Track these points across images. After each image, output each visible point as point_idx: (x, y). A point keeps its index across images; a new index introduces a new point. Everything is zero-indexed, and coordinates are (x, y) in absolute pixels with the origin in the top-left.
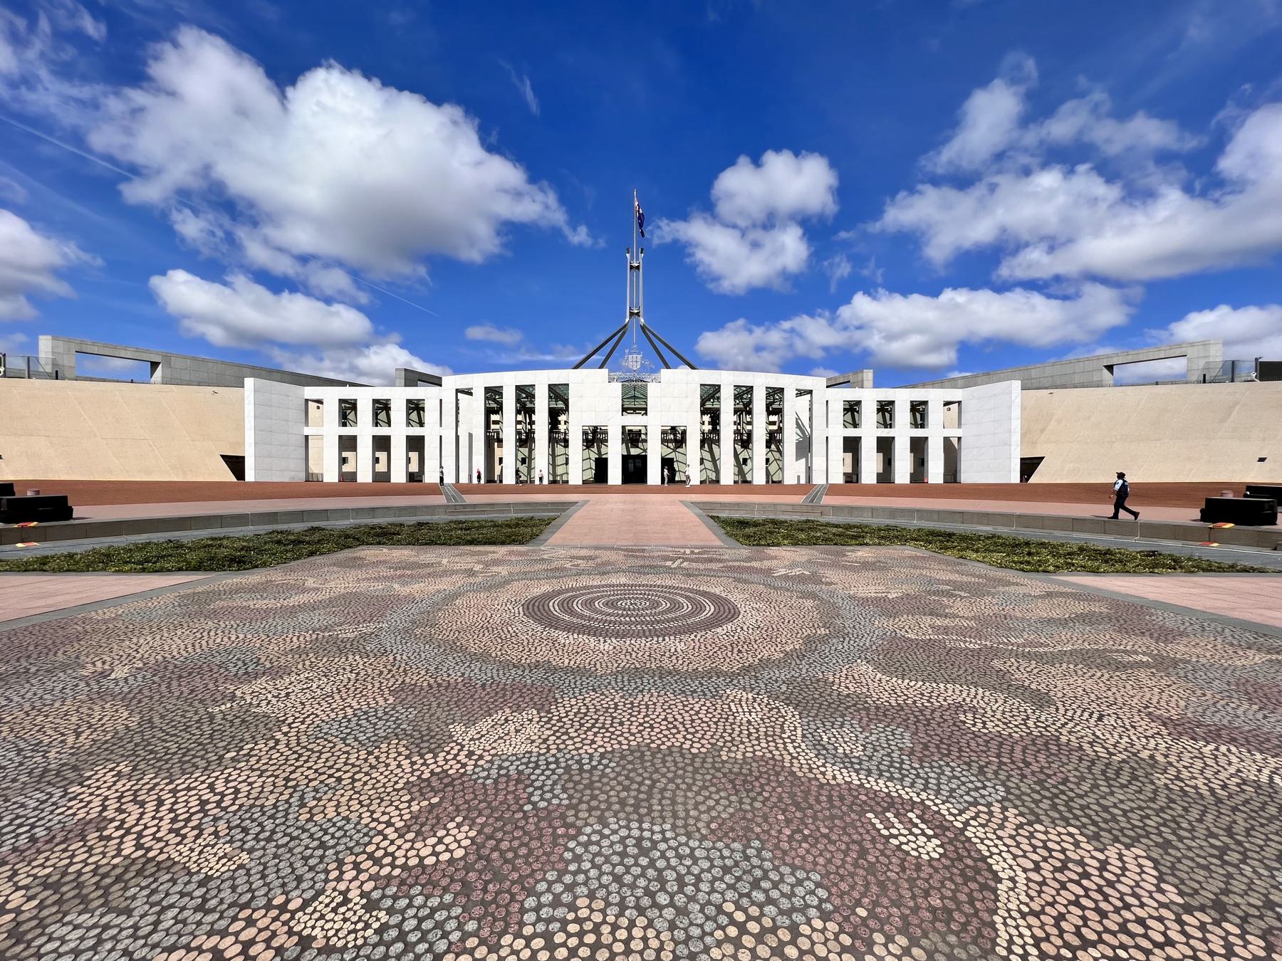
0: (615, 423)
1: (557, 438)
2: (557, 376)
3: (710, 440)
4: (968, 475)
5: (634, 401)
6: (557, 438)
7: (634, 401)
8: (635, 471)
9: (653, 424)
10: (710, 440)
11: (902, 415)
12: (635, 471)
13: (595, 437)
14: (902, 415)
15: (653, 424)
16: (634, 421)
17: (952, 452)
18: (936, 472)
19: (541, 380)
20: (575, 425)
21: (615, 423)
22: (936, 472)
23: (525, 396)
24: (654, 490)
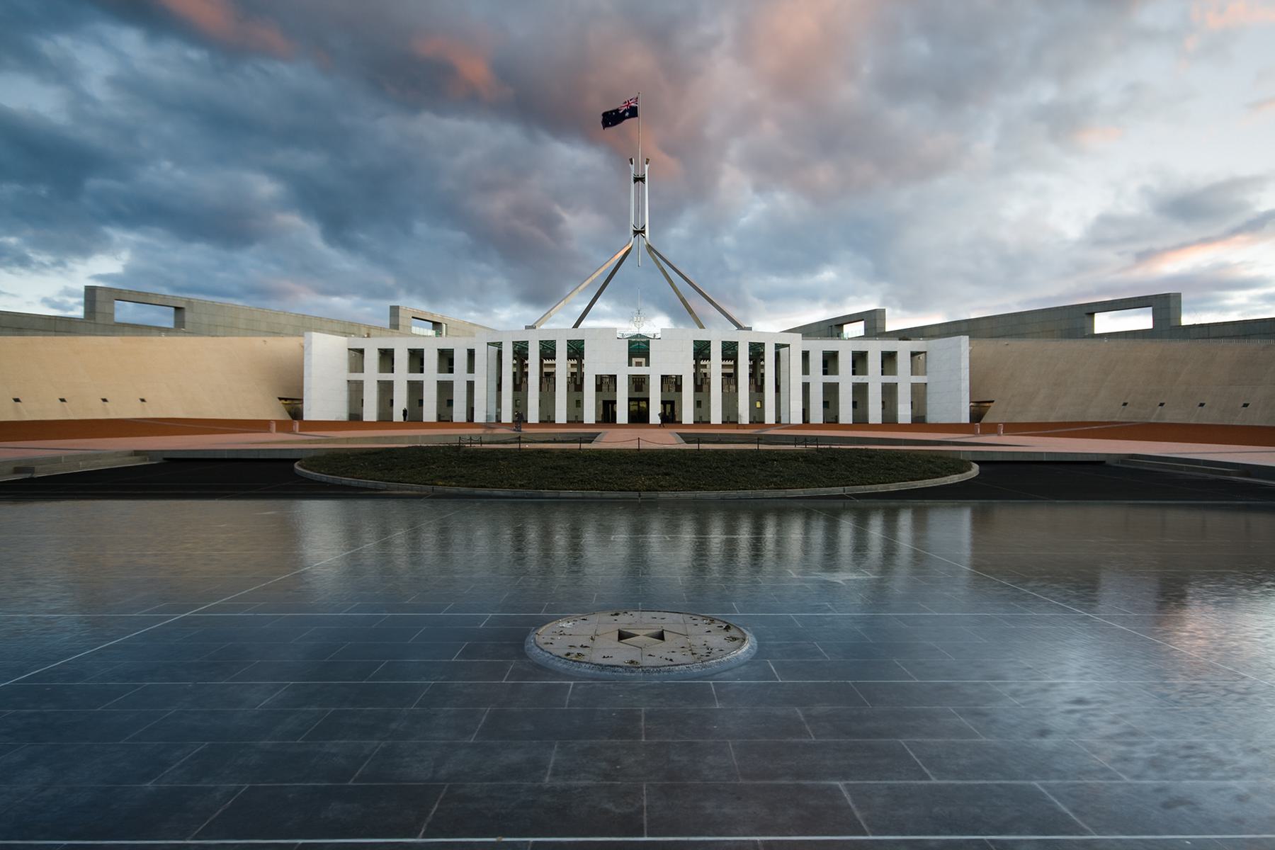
0: (624, 372)
1: (576, 383)
3: (701, 384)
6: (576, 383)
9: (654, 372)
11: (874, 363)
13: (606, 383)
14: (874, 363)
15: (654, 372)
17: (919, 393)
18: (904, 413)
21: (624, 372)
24: (655, 426)
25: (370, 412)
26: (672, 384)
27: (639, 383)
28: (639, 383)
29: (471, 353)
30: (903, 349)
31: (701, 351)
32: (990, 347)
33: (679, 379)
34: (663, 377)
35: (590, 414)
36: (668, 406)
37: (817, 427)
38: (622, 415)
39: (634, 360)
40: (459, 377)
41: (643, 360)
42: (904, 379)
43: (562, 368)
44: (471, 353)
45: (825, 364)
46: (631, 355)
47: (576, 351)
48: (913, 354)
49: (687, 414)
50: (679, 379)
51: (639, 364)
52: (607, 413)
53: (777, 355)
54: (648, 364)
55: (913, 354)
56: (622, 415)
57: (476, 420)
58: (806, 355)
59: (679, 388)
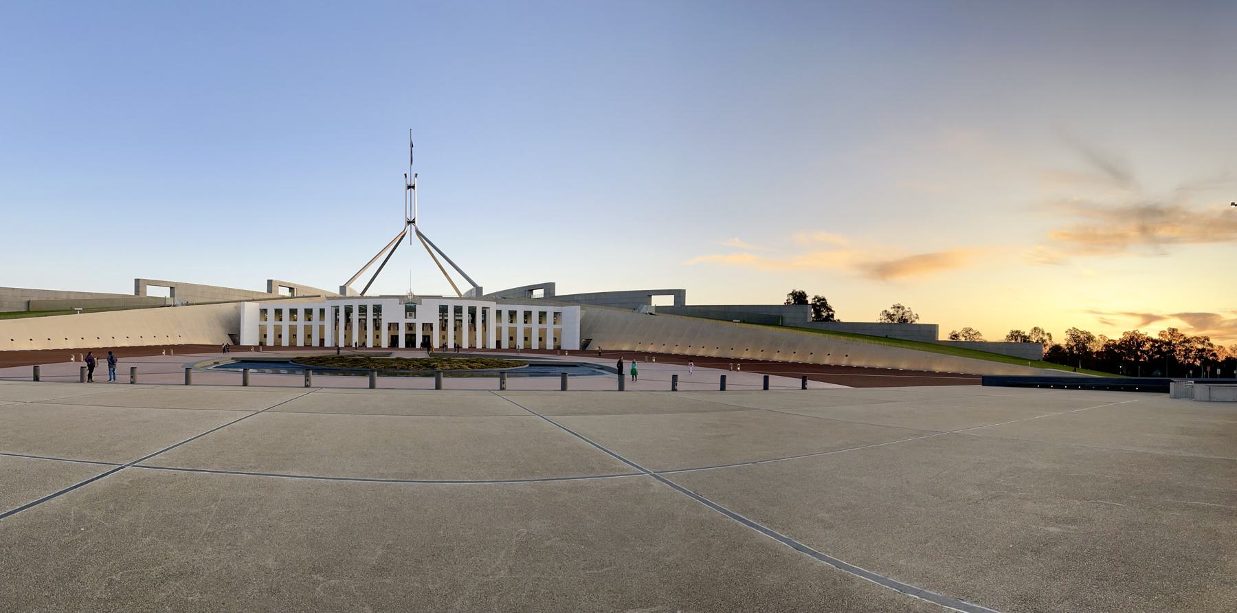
1: (377, 327)
3: (444, 327)
5: (410, 310)
6: (377, 327)
7: (410, 310)
8: (410, 342)
9: (418, 322)
10: (444, 327)
12: (410, 342)
13: (393, 326)
25: (270, 342)
26: (428, 327)
27: (411, 327)
28: (411, 327)
29: (322, 311)
30: (550, 310)
31: (444, 310)
32: (596, 311)
33: (431, 325)
35: (385, 343)
37: (505, 350)
38: (402, 343)
44: (322, 311)
47: (378, 310)
48: (556, 314)
49: (436, 343)
50: (431, 325)
53: (484, 312)
55: (556, 314)
56: (402, 343)
58: (499, 313)
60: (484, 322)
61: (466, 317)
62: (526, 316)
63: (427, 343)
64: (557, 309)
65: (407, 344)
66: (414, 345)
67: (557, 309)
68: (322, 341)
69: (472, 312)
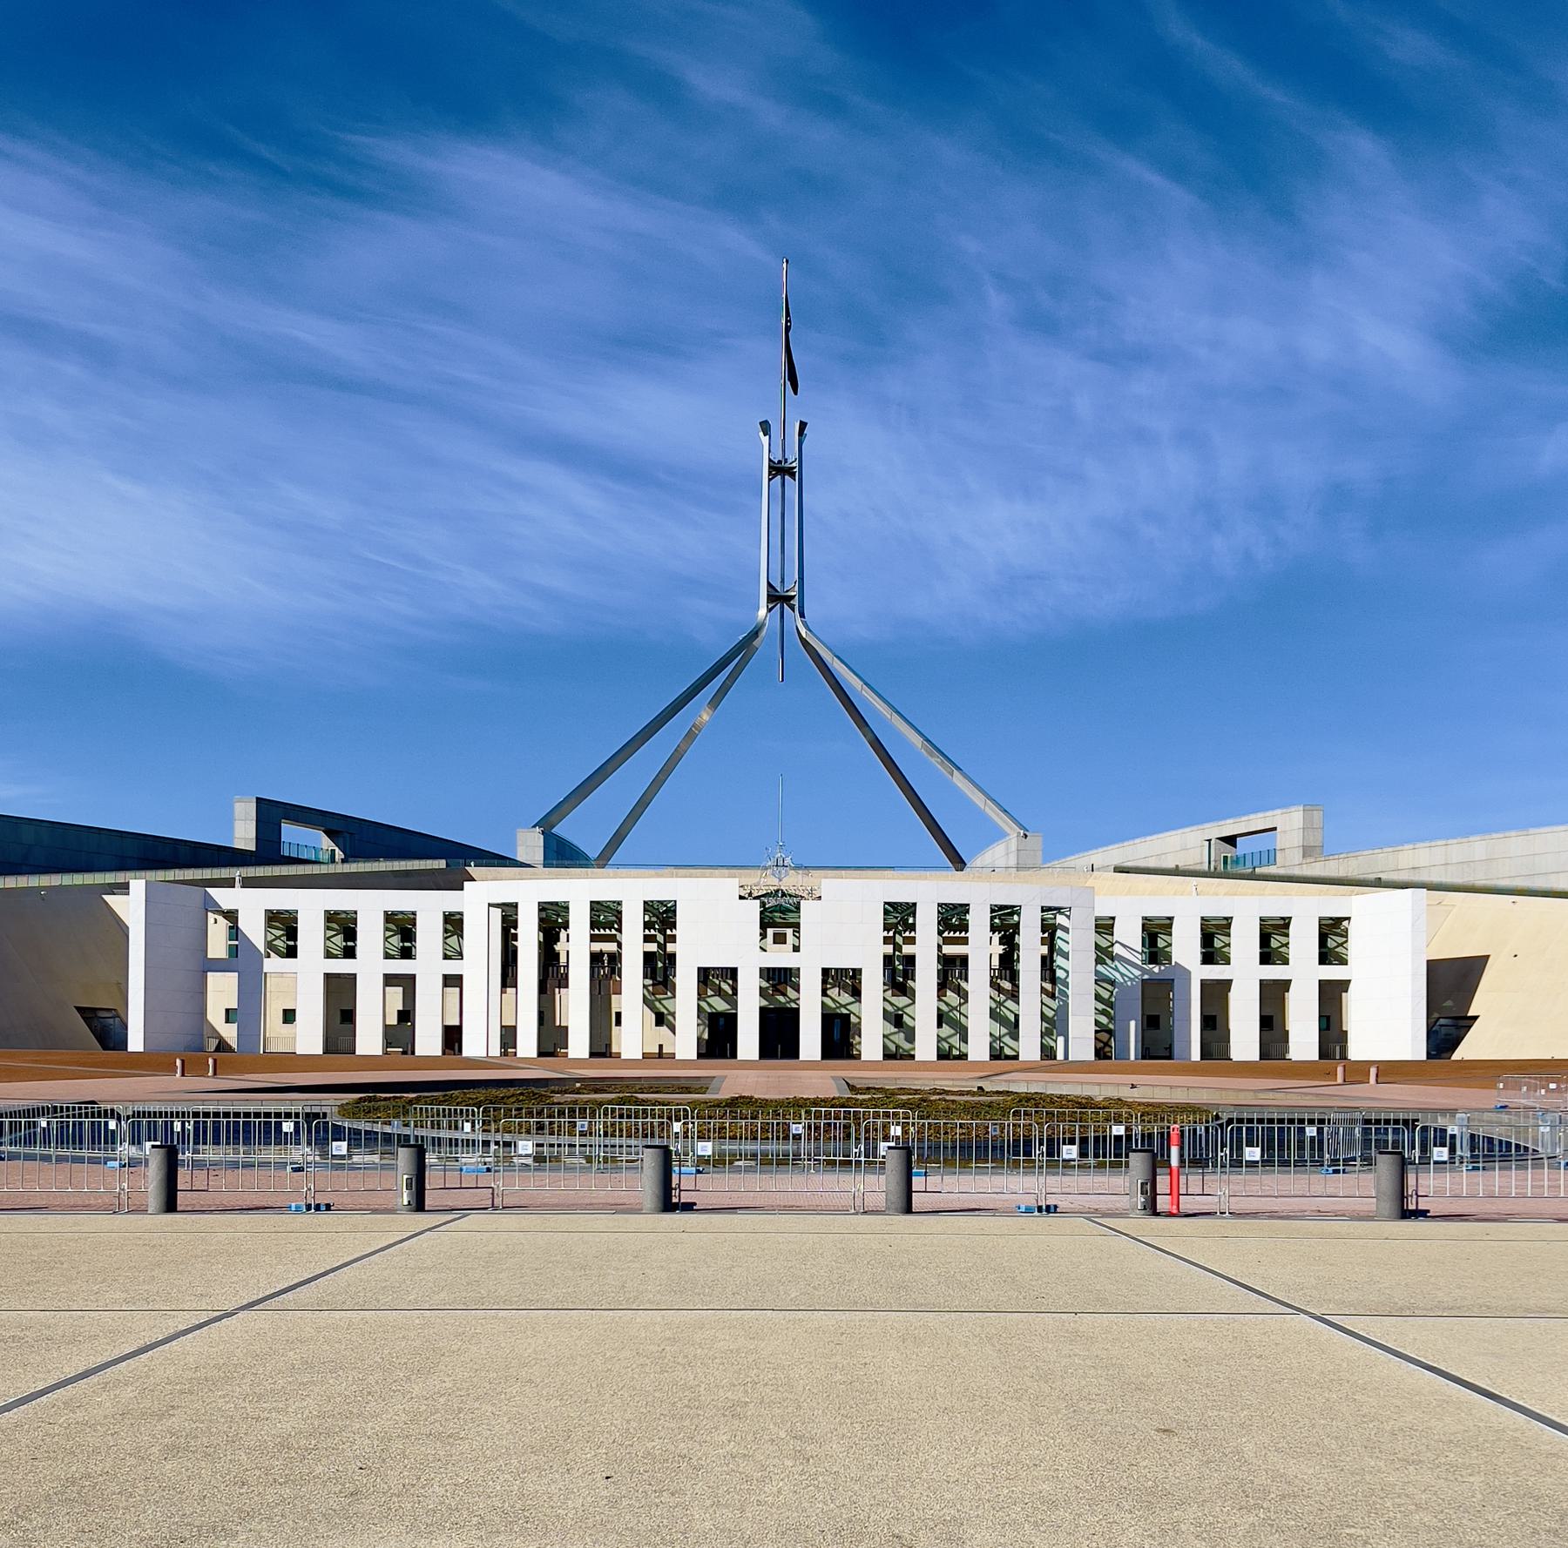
0: (752, 959)
2: (660, 887)
4: (1359, 1048)
5: (778, 917)
7: (778, 917)
8: (779, 1033)
12: (779, 1033)
13: (716, 979)
16: (780, 957)
18: (1303, 1041)
19: (632, 891)
20: (688, 960)
21: (752, 959)
22: (1303, 1041)
23: (605, 917)
24: (810, 1065)
26: (843, 980)
27: (779, 979)
28: (779, 979)
29: (453, 924)
31: (899, 917)
33: (857, 973)
34: (825, 972)
35: (686, 1040)
36: (837, 1021)
39: (770, 932)
40: (428, 964)
41: (789, 932)
42: (1303, 971)
43: (633, 946)
44: (453, 924)
45: (1265, 939)
46: (764, 926)
47: (661, 918)
49: (871, 1043)
51: (780, 939)
52: (719, 1037)
53: (1050, 931)
54: (796, 949)
57: (466, 1052)
59: (856, 993)
60: (1047, 964)
61: (982, 949)
62: (1207, 939)
63: (839, 1037)
64: (1333, 903)
65: (766, 1051)
66: (792, 1051)
67: (1333, 903)
68: (452, 1037)
69: (1005, 923)
